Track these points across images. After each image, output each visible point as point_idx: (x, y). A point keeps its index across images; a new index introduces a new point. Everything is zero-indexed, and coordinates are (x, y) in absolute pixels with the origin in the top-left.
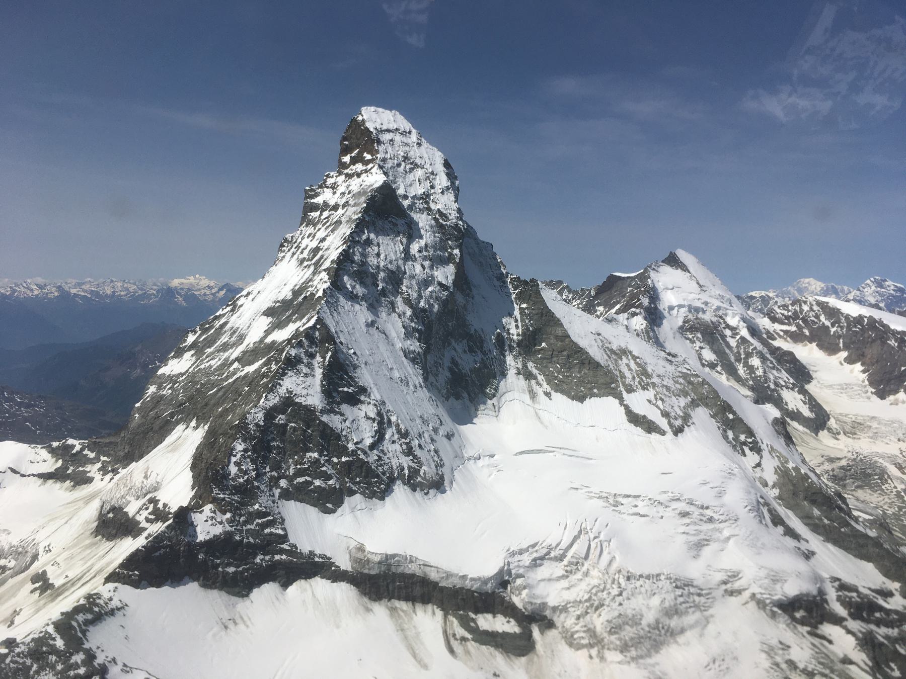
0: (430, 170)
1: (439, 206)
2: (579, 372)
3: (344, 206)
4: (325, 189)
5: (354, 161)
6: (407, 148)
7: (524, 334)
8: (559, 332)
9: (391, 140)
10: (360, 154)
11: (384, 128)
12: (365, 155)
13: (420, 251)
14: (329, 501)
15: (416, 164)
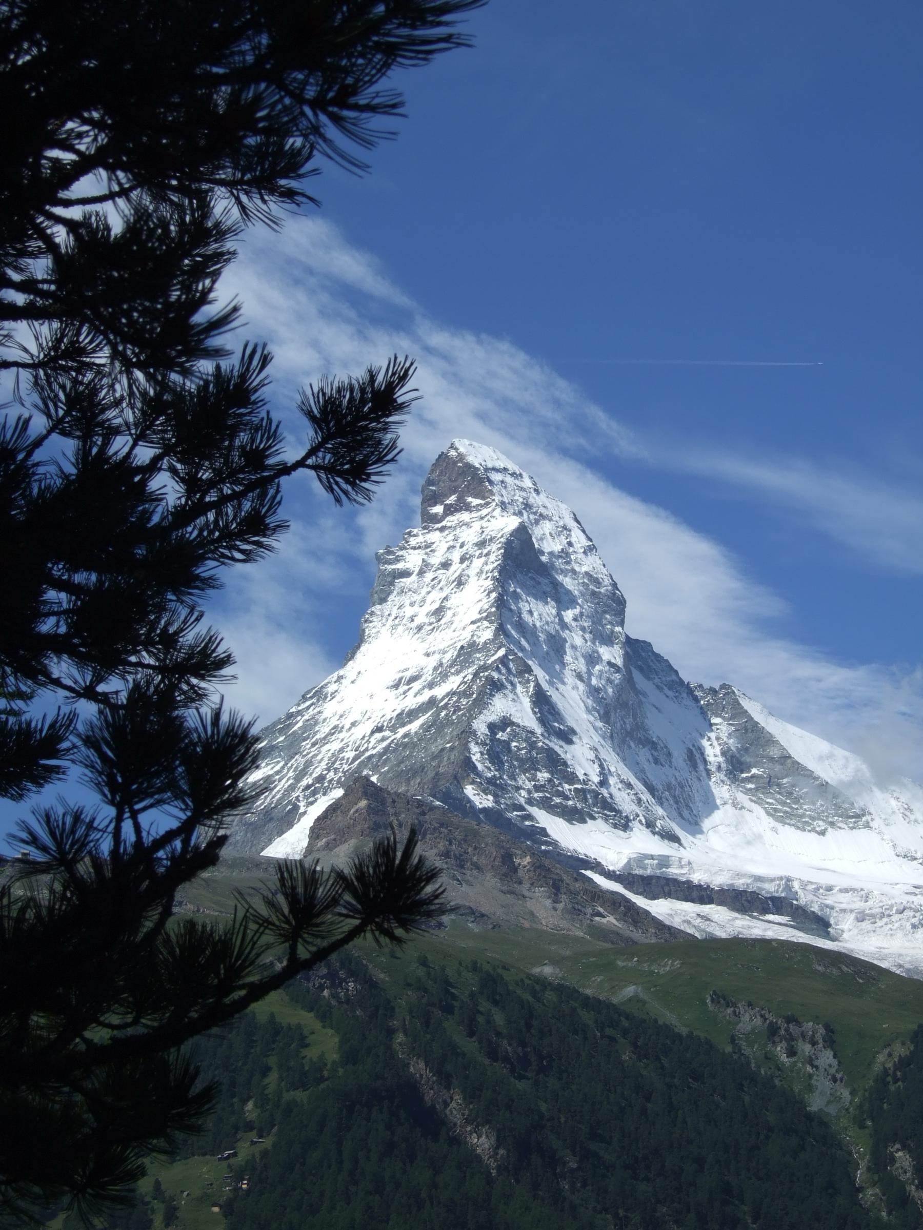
0: (561, 523)
1: (584, 569)
2: (814, 803)
3: (463, 560)
4: (411, 551)
5: (450, 510)
6: (524, 494)
7: (723, 753)
8: (774, 752)
9: (502, 482)
10: (460, 499)
11: (490, 466)
12: (470, 499)
13: (575, 619)
14: (574, 816)
15: (541, 515)
